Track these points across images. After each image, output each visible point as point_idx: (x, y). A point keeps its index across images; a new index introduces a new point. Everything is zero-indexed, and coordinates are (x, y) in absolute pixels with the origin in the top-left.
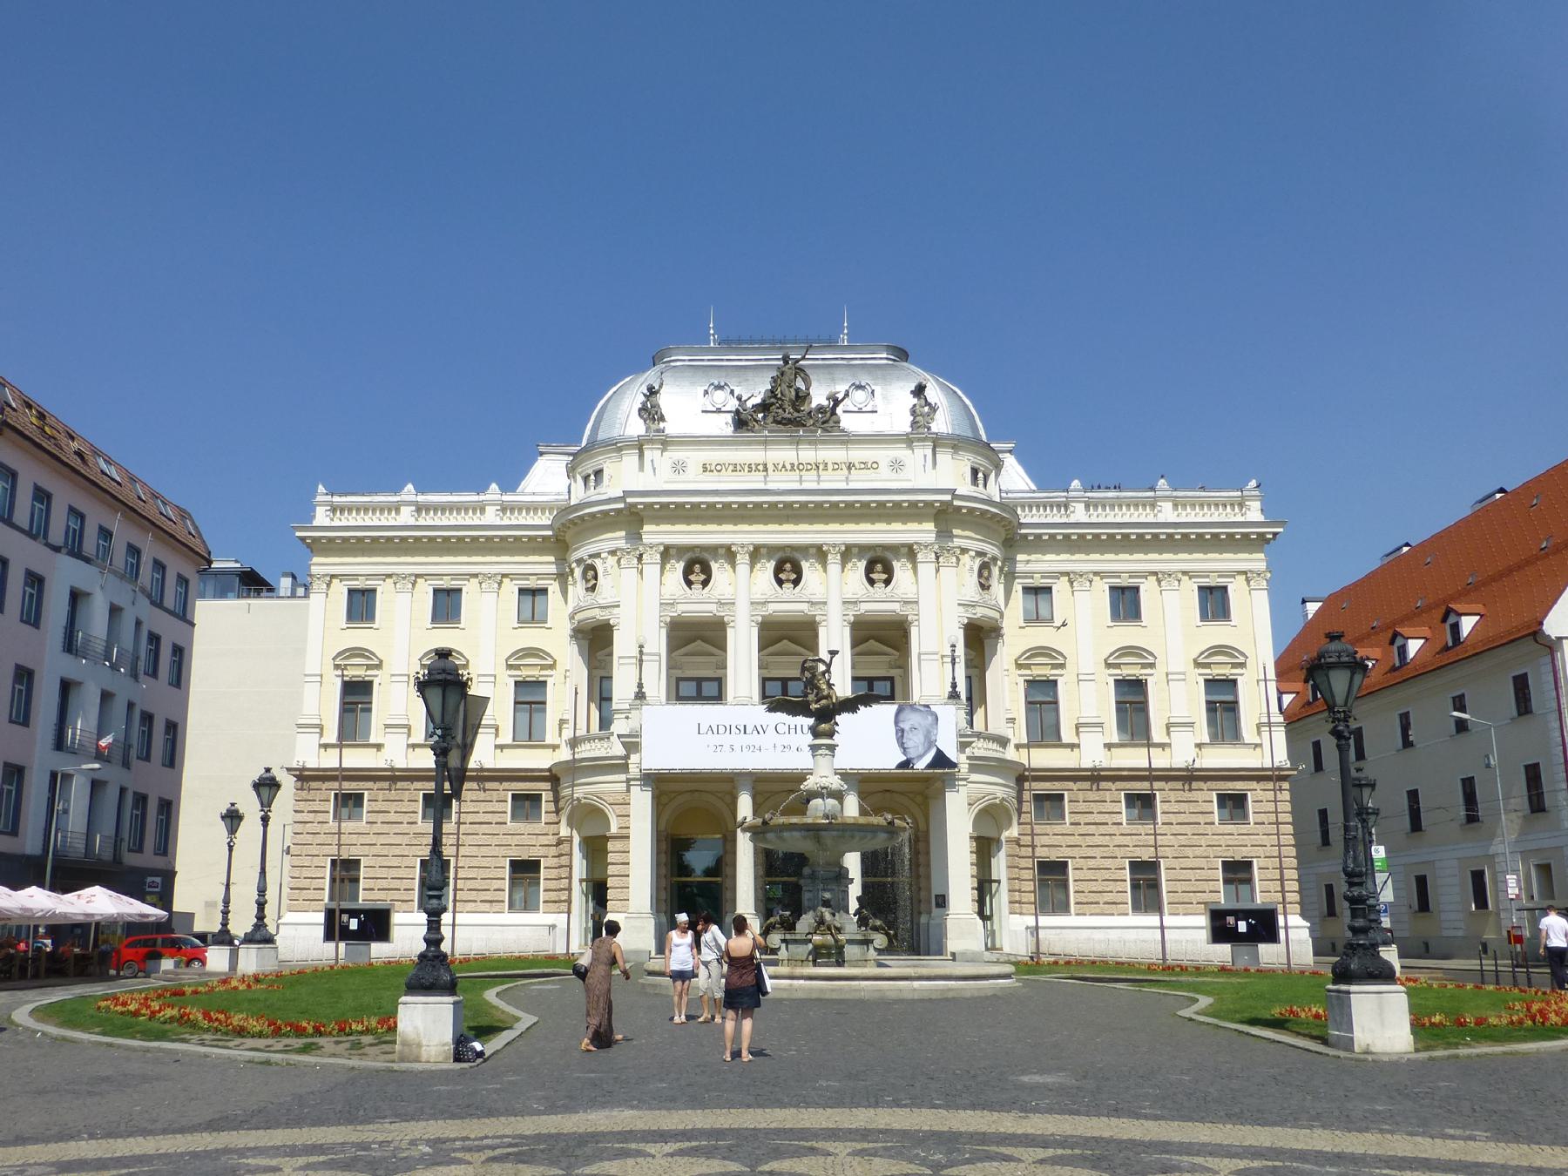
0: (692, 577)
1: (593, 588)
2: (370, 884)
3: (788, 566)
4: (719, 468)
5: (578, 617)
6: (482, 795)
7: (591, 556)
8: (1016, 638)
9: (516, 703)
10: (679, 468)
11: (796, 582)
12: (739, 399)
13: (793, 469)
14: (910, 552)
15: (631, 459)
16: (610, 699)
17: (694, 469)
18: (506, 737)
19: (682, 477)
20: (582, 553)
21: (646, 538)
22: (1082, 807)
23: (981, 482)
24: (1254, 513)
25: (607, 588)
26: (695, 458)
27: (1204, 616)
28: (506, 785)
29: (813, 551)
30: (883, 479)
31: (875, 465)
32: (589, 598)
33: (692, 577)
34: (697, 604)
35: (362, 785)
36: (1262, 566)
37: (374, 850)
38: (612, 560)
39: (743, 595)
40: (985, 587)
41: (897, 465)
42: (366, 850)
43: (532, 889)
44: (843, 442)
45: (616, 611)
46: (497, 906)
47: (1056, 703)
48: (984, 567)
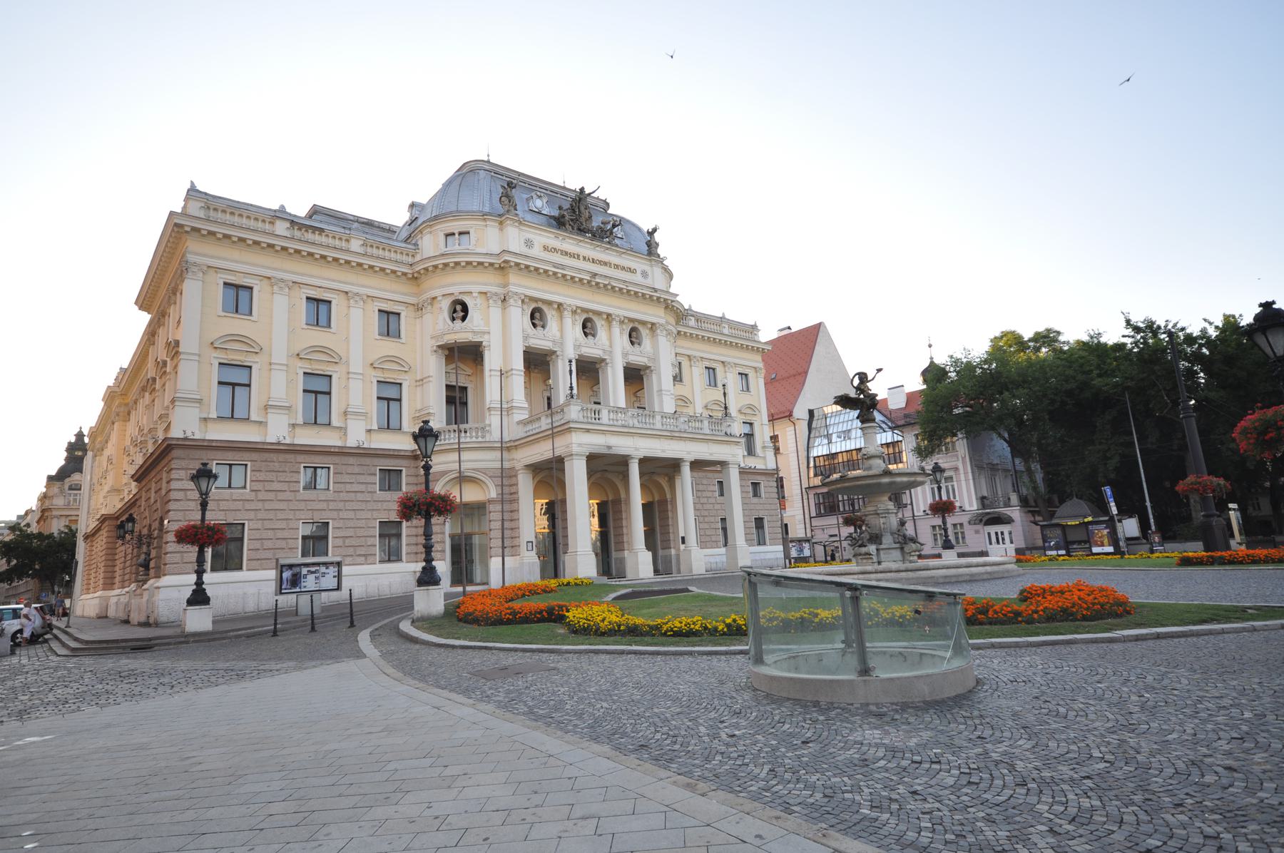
1: (464, 319)
2: (257, 545)
6: (357, 470)
14: (653, 327)
20: (455, 290)
28: (376, 461)
30: (638, 278)
31: (633, 271)
32: (458, 322)
33: (536, 322)
35: (247, 455)
36: (761, 365)
37: (261, 515)
41: (644, 274)
43: (393, 542)
45: (486, 337)
46: (370, 559)
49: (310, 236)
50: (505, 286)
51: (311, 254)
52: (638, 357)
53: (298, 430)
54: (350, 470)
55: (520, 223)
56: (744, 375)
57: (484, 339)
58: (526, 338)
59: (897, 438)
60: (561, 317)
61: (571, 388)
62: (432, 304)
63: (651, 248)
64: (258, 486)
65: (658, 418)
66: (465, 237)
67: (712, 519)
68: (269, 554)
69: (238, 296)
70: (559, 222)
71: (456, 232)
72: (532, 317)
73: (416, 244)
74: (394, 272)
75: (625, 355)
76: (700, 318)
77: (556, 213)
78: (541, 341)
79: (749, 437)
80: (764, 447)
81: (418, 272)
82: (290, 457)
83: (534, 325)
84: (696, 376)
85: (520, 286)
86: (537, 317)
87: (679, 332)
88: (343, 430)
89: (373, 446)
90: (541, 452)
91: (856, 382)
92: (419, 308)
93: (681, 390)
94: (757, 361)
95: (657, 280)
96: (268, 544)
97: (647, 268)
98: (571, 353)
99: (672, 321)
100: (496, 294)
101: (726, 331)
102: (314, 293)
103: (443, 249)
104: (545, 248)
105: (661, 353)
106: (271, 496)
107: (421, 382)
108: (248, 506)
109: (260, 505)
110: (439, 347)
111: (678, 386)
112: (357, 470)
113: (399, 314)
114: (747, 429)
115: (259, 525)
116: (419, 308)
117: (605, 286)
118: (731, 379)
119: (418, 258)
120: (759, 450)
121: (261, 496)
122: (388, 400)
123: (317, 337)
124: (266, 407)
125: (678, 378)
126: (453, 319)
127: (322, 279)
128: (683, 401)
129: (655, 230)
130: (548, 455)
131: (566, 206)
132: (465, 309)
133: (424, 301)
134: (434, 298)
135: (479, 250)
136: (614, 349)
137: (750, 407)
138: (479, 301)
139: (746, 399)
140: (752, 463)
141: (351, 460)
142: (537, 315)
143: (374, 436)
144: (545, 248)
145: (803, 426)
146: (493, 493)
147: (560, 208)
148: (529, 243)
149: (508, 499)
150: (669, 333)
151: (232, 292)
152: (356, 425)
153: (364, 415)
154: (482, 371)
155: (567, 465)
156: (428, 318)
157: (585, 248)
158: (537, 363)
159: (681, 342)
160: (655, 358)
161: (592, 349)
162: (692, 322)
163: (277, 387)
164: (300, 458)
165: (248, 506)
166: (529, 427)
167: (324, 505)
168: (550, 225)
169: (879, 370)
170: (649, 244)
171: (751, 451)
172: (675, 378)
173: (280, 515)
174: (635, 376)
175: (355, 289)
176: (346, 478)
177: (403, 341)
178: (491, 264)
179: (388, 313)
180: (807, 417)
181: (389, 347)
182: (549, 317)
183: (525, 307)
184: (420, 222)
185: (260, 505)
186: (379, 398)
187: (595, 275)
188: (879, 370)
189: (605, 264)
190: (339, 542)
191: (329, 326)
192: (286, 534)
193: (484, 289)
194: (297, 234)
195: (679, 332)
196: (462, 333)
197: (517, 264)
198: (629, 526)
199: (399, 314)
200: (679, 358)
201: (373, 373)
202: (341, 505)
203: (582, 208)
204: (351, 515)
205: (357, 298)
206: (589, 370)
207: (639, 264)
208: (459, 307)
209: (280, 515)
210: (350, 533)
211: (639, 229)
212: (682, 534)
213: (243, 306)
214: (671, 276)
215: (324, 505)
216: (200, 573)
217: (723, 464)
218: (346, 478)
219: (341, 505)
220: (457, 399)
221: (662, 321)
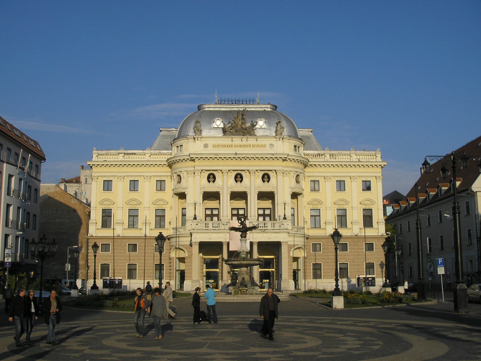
0: (209, 179)
3: (239, 176)
4: (219, 146)
5: (175, 191)
8: (308, 196)
9: (156, 216)
10: (206, 146)
11: (241, 181)
12: (224, 124)
16: (185, 215)
17: (210, 146)
18: (153, 225)
19: (207, 149)
21: (196, 168)
23: (297, 150)
24: (379, 159)
26: (210, 142)
27: (363, 190)
31: (264, 146)
32: (179, 185)
34: (211, 188)
38: (185, 173)
39: (225, 185)
40: (298, 182)
45: (187, 190)
47: (319, 216)
48: (298, 176)
69: (108, 185)
85: (200, 166)
86: (211, 178)
104: (214, 146)
127: (133, 173)
142: (211, 176)
144: (214, 146)
152: (147, 229)
163: (120, 216)
177: (166, 191)
181: (160, 195)
199: (165, 180)
216: (95, 278)
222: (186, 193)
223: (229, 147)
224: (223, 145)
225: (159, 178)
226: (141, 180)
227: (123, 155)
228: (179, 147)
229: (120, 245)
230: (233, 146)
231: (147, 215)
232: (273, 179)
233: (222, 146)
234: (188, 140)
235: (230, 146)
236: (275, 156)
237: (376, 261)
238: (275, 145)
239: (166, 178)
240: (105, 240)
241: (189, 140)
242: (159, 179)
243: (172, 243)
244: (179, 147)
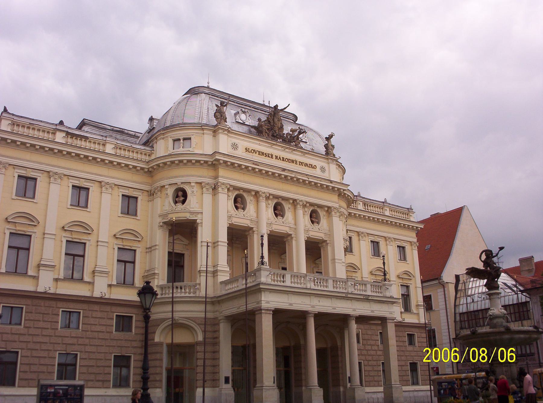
1: (183, 202)
2: (26, 368)
7: (182, 183)
13: (283, 160)
14: (329, 210)
15: (208, 137)
22: (366, 337)
25: (192, 202)
28: (114, 309)
29: (291, 201)
30: (317, 172)
31: (314, 167)
32: (179, 205)
33: (238, 205)
35: (23, 301)
36: (415, 240)
37: (31, 346)
38: (196, 189)
41: (323, 169)
42: (24, 345)
44: (302, 152)
45: (199, 216)
49: (79, 143)
50: (216, 177)
51: (78, 155)
52: (317, 232)
53: (60, 284)
54: (94, 314)
55: (229, 132)
56: (402, 249)
57: (198, 218)
58: (230, 217)
59: (528, 300)
60: (258, 201)
61: (262, 257)
62: (161, 191)
63: (329, 148)
64: (31, 324)
65: (330, 282)
66: (187, 142)
67: (375, 363)
68: (34, 376)
70: (259, 131)
71: (181, 138)
72: (235, 201)
73: (152, 147)
74: (135, 167)
75: (307, 231)
76: (367, 203)
77: (256, 124)
78: (242, 219)
79: (406, 297)
80: (418, 306)
81: (152, 167)
82: (53, 303)
83: (237, 208)
84: (363, 247)
86: (239, 202)
87: (350, 214)
88: (92, 284)
89: (113, 297)
90: (236, 307)
91: (484, 257)
92: (151, 194)
93: (351, 259)
94: (412, 237)
95: (334, 174)
96: (34, 368)
97: (325, 165)
98: (265, 231)
99: (344, 205)
100: (208, 184)
101: (387, 213)
102: (77, 183)
103: (171, 151)
104: (247, 150)
105: (337, 230)
106: (38, 332)
107: (150, 249)
108: (22, 338)
109: (30, 339)
110: (164, 223)
111: (349, 256)
112: (99, 315)
113: (137, 198)
114: (404, 291)
115: (29, 353)
116: (151, 194)
117: (292, 178)
118: (390, 252)
119: (153, 157)
120: (414, 309)
121: (32, 331)
122: (125, 262)
123: (79, 215)
124: (39, 266)
125: (349, 250)
126: (176, 202)
127: (84, 172)
128: (352, 268)
129: (331, 136)
130: (243, 309)
131: (264, 118)
132: (185, 195)
133: (156, 189)
134: (164, 186)
135: (196, 152)
136: (299, 227)
137: (407, 273)
138: (195, 189)
139: (403, 267)
140: (409, 319)
141: (96, 307)
142: (239, 199)
143: (114, 289)
145: (451, 289)
146: (200, 338)
147: (259, 120)
148: (235, 146)
149: (212, 342)
150: (342, 214)
151: (23, 181)
153: (107, 273)
154: (196, 242)
155: (257, 317)
156: (158, 201)
157: (277, 150)
158: (238, 237)
159: (351, 221)
160: (331, 233)
161: (281, 226)
162: (361, 206)
164: (60, 304)
165: (22, 338)
166: (229, 286)
167: (74, 341)
168: (250, 132)
169: (501, 248)
170: (326, 146)
171: (407, 308)
172: (346, 250)
173: (44, 347)
174: (315, 250)
175: (106, 180)
176: (92, 321)
178: (206, 162)
179: (129, 197)
180: (454, 281)
181: (128, 223)
182: (248, 201)
183: (230, 194)
184: (156, 130)
185: (30, 339)
186: (118, 261)
187: (284, 170)
188: (501, 248)
189: (293, 161)
190: (84, 370)
191: (86, 207)
192: (47, 361)
193: (199, 180)
194: (70, 140)
195: (350, 214)
196: (181, 213)
197: (225, 162)
198: (306, 368)
199: (137, 198)
200: (350, 234)
201: (116, 241)
202: (87, 341)
203: (276, 120)
204: (93, 349)
205: (108, 186)
206: (278, 244)
207: (319, 163)
208: (180, 193)
209: (44, 347)
210: (92, 363)
211: (320, 136)
212: (348, 375)
213: (29, 193)
214: (344, 171)
215: (74, 341)
217: (383, 320)
218: (92, 321)
219: (87, 341)
220: (177, 264)
221: (336, 205)
222: (198, 221)
223: (269, 157)
224: (259, 152)
225: (127, 191)
226: (94, 190)
227: (64, 134)
228: (182, 141)
229: (46, 312)
230: (274, 157)
231: (102, 257)
232: (324, 221)
233: (258, 153)
234: (202, 132)
235: (270, 156)
236: (333, 185)
237: (363, 360)
238: (327, 168)
239: (140, 194)
240: (12, 300)
241: (205, 131)
242: (127, 192)
243: (156, 315)
244: (182, 141)
